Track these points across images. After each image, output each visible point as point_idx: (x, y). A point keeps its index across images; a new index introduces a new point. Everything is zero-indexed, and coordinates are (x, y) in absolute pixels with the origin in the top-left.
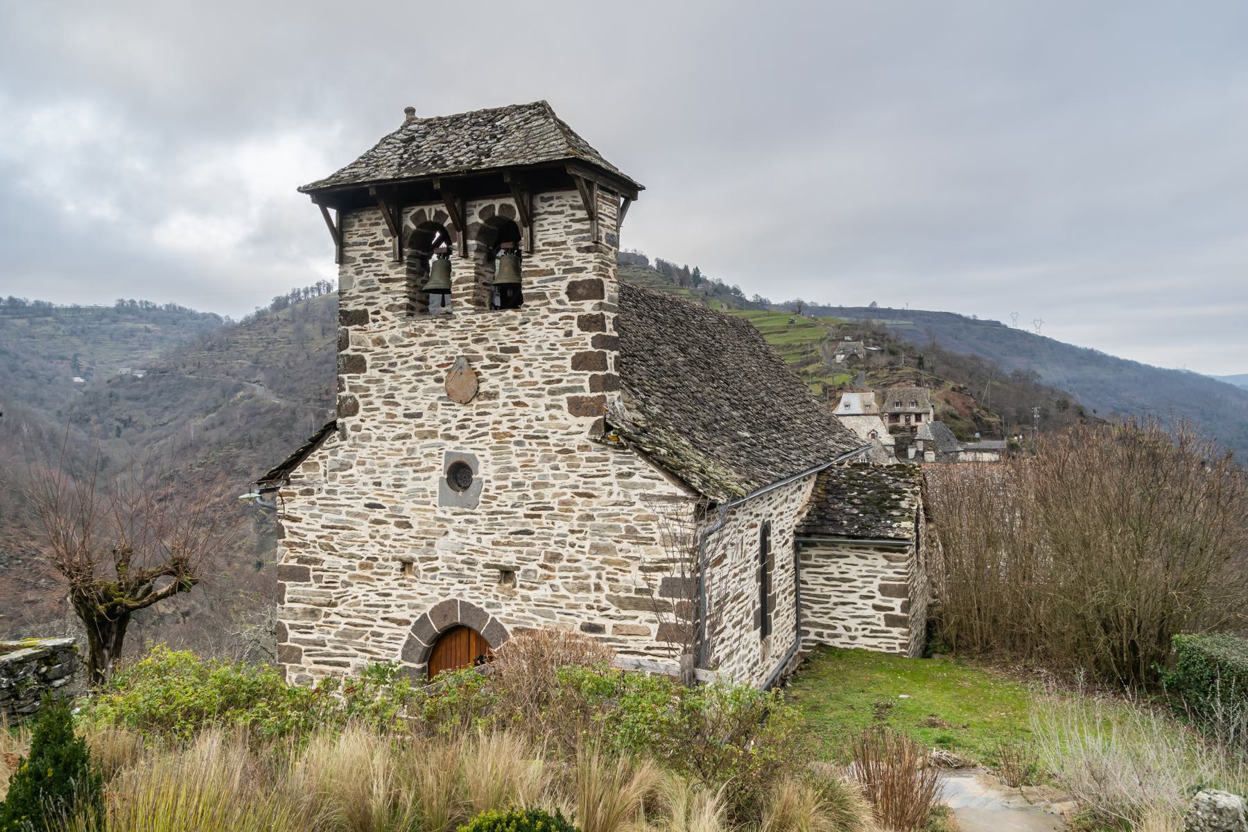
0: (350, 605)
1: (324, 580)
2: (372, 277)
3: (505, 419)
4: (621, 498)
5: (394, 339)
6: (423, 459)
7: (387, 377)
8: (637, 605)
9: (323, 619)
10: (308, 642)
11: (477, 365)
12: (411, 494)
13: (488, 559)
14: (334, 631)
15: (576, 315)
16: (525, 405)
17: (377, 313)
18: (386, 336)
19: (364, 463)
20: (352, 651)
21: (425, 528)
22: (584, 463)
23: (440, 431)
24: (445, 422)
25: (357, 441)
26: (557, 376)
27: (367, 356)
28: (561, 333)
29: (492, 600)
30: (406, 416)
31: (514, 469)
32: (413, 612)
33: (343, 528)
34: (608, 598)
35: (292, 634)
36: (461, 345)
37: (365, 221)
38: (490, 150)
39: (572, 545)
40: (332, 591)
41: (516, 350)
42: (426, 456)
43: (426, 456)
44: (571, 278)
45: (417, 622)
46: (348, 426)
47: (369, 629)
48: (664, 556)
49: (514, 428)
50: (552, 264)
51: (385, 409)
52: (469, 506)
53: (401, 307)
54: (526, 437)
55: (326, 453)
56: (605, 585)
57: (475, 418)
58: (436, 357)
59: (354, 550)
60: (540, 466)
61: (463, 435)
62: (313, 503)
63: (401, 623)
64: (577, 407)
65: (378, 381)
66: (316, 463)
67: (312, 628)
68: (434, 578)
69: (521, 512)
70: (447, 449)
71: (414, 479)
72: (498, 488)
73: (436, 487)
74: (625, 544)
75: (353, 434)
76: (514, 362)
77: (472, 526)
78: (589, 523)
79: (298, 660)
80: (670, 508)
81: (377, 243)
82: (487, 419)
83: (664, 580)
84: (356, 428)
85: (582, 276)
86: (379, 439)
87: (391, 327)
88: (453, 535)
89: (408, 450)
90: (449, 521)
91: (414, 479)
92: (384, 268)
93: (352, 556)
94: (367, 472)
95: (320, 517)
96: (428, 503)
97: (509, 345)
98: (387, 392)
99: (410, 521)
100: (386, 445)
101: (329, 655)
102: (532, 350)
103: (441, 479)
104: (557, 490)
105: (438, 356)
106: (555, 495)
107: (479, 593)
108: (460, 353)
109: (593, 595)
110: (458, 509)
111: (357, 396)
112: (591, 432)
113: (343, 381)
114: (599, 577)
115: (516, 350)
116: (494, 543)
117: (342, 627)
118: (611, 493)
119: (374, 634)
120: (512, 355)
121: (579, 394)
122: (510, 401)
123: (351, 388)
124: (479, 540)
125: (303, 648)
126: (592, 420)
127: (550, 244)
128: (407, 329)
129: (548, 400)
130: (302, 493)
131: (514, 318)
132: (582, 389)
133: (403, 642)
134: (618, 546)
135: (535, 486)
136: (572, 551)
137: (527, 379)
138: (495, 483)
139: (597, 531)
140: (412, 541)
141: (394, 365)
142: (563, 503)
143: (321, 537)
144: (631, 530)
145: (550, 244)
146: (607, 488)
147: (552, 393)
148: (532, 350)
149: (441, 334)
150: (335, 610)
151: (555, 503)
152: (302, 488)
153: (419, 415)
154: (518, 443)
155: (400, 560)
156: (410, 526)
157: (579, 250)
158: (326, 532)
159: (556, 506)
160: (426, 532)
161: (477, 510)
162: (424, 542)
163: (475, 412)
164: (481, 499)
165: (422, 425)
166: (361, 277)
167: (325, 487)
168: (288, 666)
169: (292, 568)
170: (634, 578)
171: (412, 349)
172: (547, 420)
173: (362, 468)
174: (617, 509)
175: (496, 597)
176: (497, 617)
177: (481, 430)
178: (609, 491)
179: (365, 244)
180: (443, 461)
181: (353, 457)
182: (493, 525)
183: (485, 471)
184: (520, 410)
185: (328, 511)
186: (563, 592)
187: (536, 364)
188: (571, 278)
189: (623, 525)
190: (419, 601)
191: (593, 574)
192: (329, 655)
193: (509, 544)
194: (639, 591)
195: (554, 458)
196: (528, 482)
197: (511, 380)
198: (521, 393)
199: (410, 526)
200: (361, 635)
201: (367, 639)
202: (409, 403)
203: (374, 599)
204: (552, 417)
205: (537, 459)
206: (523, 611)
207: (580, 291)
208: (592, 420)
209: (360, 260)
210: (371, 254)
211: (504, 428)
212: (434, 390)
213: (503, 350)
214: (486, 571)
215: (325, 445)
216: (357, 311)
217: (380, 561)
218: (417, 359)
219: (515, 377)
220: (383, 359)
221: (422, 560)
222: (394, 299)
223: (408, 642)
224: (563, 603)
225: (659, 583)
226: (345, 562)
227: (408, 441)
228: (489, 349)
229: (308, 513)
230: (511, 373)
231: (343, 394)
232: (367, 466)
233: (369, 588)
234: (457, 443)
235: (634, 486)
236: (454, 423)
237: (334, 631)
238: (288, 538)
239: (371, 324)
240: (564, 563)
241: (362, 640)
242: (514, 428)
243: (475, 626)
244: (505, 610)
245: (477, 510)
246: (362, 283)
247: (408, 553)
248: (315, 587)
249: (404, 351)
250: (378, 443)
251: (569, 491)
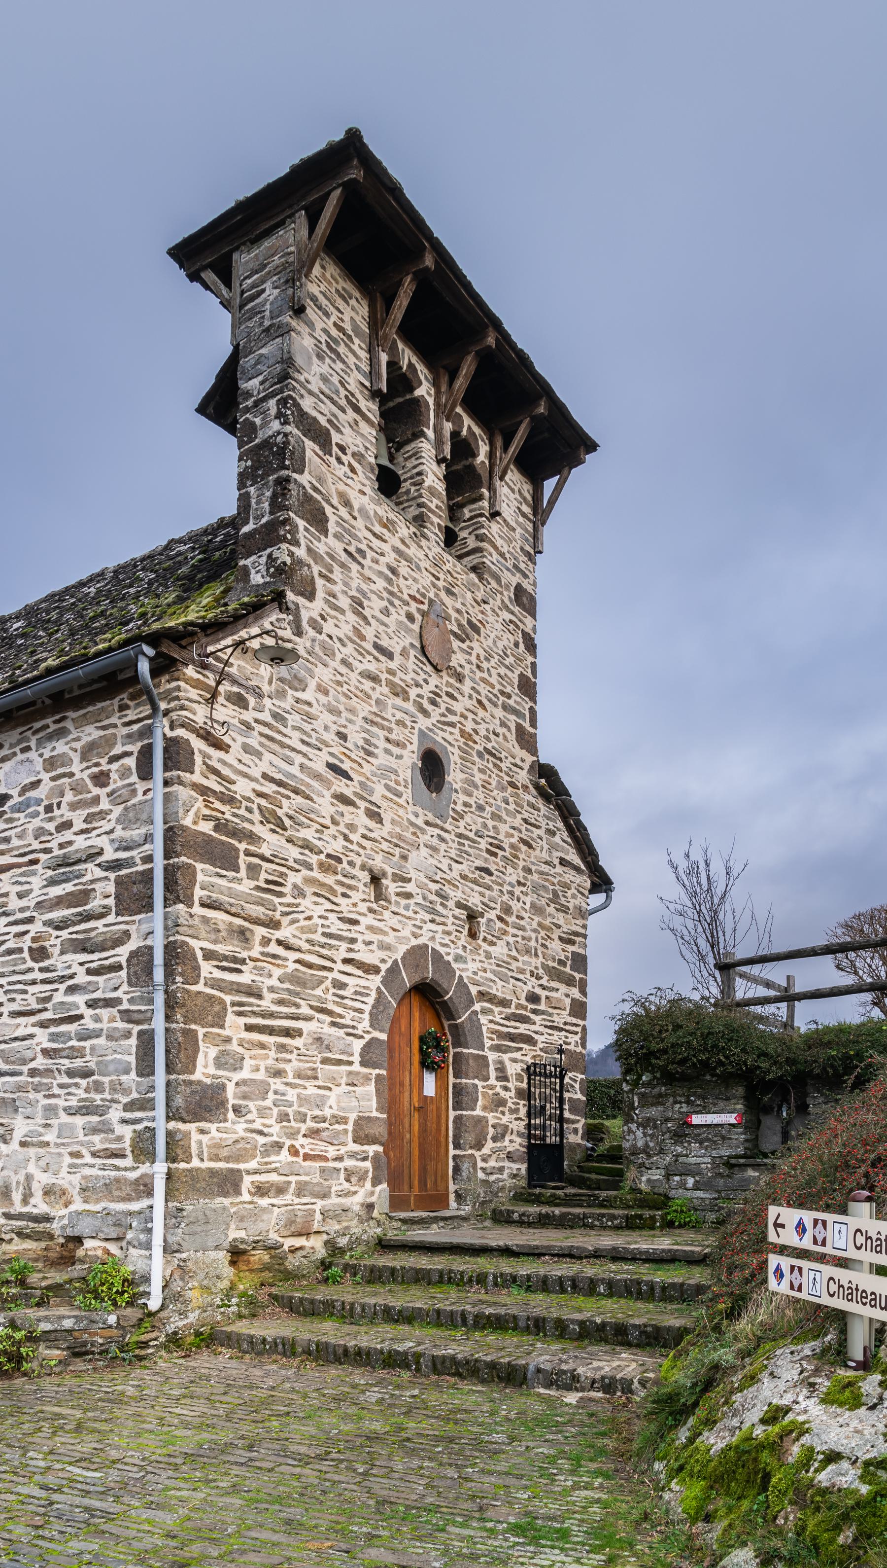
0: (302, 930)
1: (263, 876)
9: (261, 949)
10: (238, 989)
14: (277, 972)
20: (305, 1010)
29: (460, 951)
32: (383, 954)
33: (296, 791)
35: (207, 969)
40: (277, 900)
45: (389, 971)
59: (308, 834)
63: (370, 969)
67: (243, 962)
93: (306, 845)
96: (399, 795)
101: (272, 1015)
103: (414, 765)
117: (292, 966)
125: (228, 999)
133: (371, 1000)
143: (260, 795)
155: (371, 871)
158: (269, 788)
162: (397, 851)
168: (201, 1031)
169: (208, 840)
176: (464, 975)
190: (390, 939)
192: (272, 1015)
196: (488, 808)
203: (336, 926)
206: (485, 971)
226: (294, 852)
233: (329, 906)
237: (277, 972)
241: (318, 992)
244: (472, 966)
248: (246, 886)
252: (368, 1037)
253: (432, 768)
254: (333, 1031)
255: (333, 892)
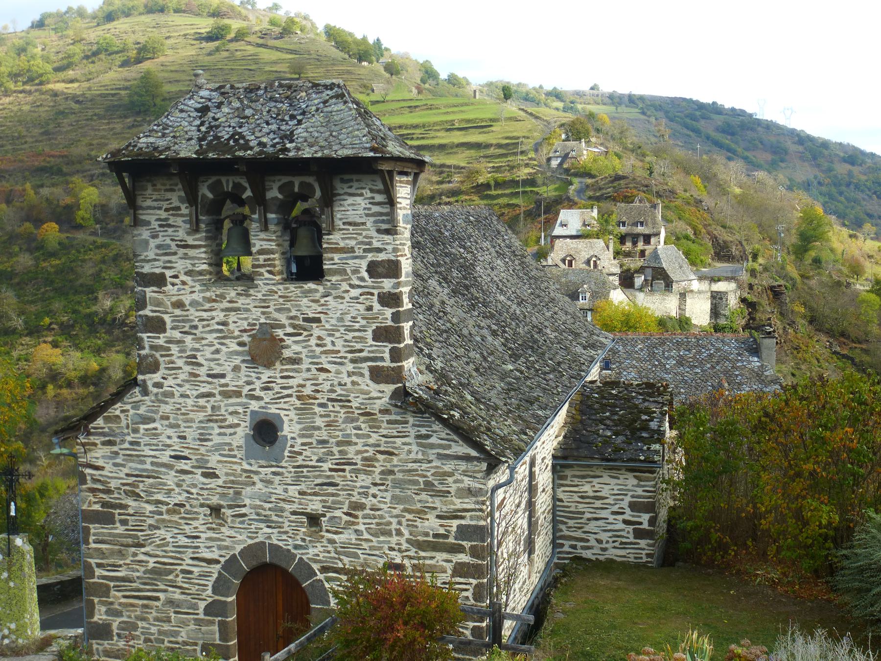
0: (158, 546)
2: (168, 241)
3: (309, 383)
4: (420, 456)
5: (194, 303)
6: (228, 416)
7: (188, 339)
8: (435, 547)
9: (132, 559)
11: (280, 333)
12: (218, 447)
13: (295, 507)
14: (143, 569)
15: (376, 292)
16: (327, 371)
17: (176, 277)
18: (187, 299)
19: (168, 418)
20: (162, 587)
21: (232, 478)
22: (385, 425)
23: (245, 391)
24: (249, 383)
25: (160, 397)
26: (358, 346)
27: (167, 318)
28: (361, 308)
29: (299, 543)
30: (209, 376)
31: (319, 428)
32: (223, 552)
33: (148, 477)
34: (408, 541)
35: (98, 572)
36: (263, 313)
37: (159, 186)
38: (292, 132)
39: (374, 496)
40: (140, 534)
41: (318, 320)
42: (231, 414)
43: (231, 414)
44: (370, 257)
45: (226, 562)
46: (150, 384)
47: (179, 568)
48: (459, 506)
49: (318, 391)
50: (352, 243)
51: (188, 368)
52: (276, 460)
53: (201, 273)
54: (328, 399)
55: (128, 407)
56: (406, 532)
57: (279, 381)
58: (237, 324)
59: (160, 497)
60: (344, 426)
61: (267, 396)
62: (117, 453)
63: (210, 562)
64: (377, 375)
65: (179, 342)
66: (118, 417)
67: (120, 566)
68: (242, 522)
69: (326, 466)
70: (252, 408)
71: (220, 434)
72: (303, 444)
73: (242, 442)
74: (424, 496)
75: (155, 390)
76: (317, 332)
77: (278, 478)
78: (390, 477)
79: (107, 593)
80: (463, 466)
81: (173, 209)
82: (291, 382)
83: (458, 527)
84: (158, 385)
85: (382, 257)
86: (182, 396)
87: (192, 292)
88: (259, 485)
89: (213, 408)
90: (257, 473)
91: (220, 434)
92: (181, 234)
93: (159, 502)
94: (171, 426)
95: (123, 466)
96: (235, 456)
97: (311, 315)
98: (189, 353)
99: (217, 472)
100: (190, 402)
102: (334, 322)
103: (247, 435)
104: (359, 447)
105: (240, 322)
106: (358, 452)
107: (288, 536)
108: (263, 321)
109: (394, 539)
110: (263, 463)
111: (157, 355)
112: (391, 398)
113: (142, 339)
114: (400, 523)
115: (318, 320)
116: (300, 493)
117: (151, 565)
118: (410, 452)
119: (184, 571)
120: (314, 325)
121: (380, 364)
122: (313, 367)
123: (152, 347)
124: (286, 491)
125: (112, 584)
126: (392, 387)
127: (350, 224)
128: (208, 294)
129: (350, 367)
130: (104, 443)
131: (316, 291)
132: (382, 359)
134: (417, 498)
135: (338, 444)
136: (374, 501)
137: (330, 347)
138: (300, 441)
139: (397, 484)
140: (219, 490)
141: (196, 327)
142: (365, 459)
143: (124, 485)
144: (429, 484)
145: (350, 224)
146: (406, 448)
147: (353, 361)
148: (334, 322)
149: (242, 302)
150: (143, 550)
151: (358, 459)
152: (103, 439)
153: (223, 376)
154: (322, 405)
155: (209, 506)
156: (217, 477)
157: (379, 231)
158: (131, 480)
159: (359, 462)
160: (233, 482)
161: (283, 464)
162: (231, 491)
163: (278, 375)
164: (286, 454)
165: (227, 385)
166: (158, 241)
167: (129, 438)
168: (96, 600)
170: (432, 524)
171: (214, 313)
172: (349, 386)
173: (166, 422)
174: (415, 466)
175: (303, 540)
176: (304, 557)
177: (286, 392)
178: (408, 448)
179: (160, 208)
180: (248, 418)
181: (156, 412)
182: (298, 479)
183: (290, 429)
184: (324, 375)
185: (133, 461)
186: (366, 536)
187: (337, 334)
188: (370, 257)
189: (421, 480)
191: (394, 521)
193: (315, 494)
194: (436, 536)
195: (357, 420)
196: (331, 440)
197: (315, 348)
198: (324, 361)
199: (217, 477)
200: (171, 572)
201: (177, 576)
202: (212, 364)
204: (354, 383)
205: (341, 420)
206: (329, 552)
207: (380, 270)
208: (392, 387)
209: (155, 225)
210: (166, 219)
211: (308, 391)
212: (237, 353)
213: (305, 320)
214: (293, 517)
215: (125, 399)
216: (154, 274)
217: (188, 507)
218: (218, 324)
219: (318, 345)
220: (183, 321)
221: (230, 507)
222: (193, 265)
223: (217, 578)
224: (365, 545)
225: (454, 529)
226: (149, 508)
227: (212, 399)
228: (292, 318)
229: (111, 462)
230: (313, 341)
231: (143, 352)
232: (171, 421)
233: (176, 531)
234: (262, 403)
235: (432, 446)
236: (258, 385)
238: (90, 485)
239: (170, 287)
240: (367, 511)
241: (170, 577)
242: (318, 391)
243: (283, 565)
244: (312, 551)
245: (283, 464)
246: (159, 247)
247: (215, 500)
248: (120, 529)
249: (205, 315)
250: (181, 400)
251: (371, 450)
252: (210, 600)
253: (266, 431)
254: (183, 597)
255: (180, 524)
